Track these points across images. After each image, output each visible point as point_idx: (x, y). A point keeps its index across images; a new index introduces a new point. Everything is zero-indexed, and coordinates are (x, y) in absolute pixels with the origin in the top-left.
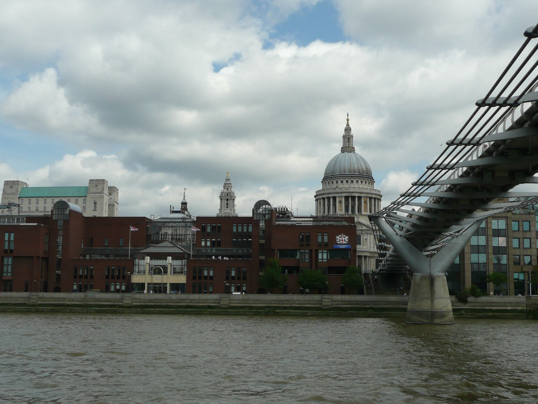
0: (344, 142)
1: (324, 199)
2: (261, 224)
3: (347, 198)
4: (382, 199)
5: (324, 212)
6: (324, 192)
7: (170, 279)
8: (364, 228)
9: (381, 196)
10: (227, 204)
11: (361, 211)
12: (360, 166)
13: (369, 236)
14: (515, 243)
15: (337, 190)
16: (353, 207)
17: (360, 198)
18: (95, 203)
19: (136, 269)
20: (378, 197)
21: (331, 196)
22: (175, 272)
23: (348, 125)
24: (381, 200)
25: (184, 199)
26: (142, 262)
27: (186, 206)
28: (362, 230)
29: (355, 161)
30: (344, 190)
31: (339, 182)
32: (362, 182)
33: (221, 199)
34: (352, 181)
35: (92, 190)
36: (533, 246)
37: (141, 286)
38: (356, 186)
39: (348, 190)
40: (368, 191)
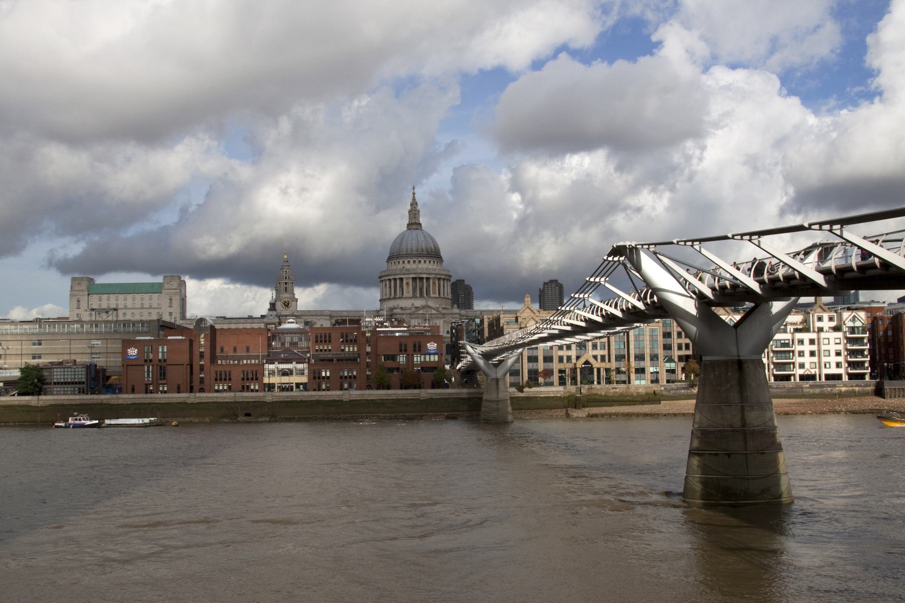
0: (410, 218)
1: (390, 280)
7: (294, 379)
8: (434, 312)
16: (421, 290)
17: (428, 279)
18: (171, 300)
19: (266, 373)
22: (297, 374)
23: (414, 199)
26: (272, 367)
29: (423, 238)
31: (406, 262)
34: (420, 262)
35: (166, 286)
37: (271, 387)
40: (437, 271)
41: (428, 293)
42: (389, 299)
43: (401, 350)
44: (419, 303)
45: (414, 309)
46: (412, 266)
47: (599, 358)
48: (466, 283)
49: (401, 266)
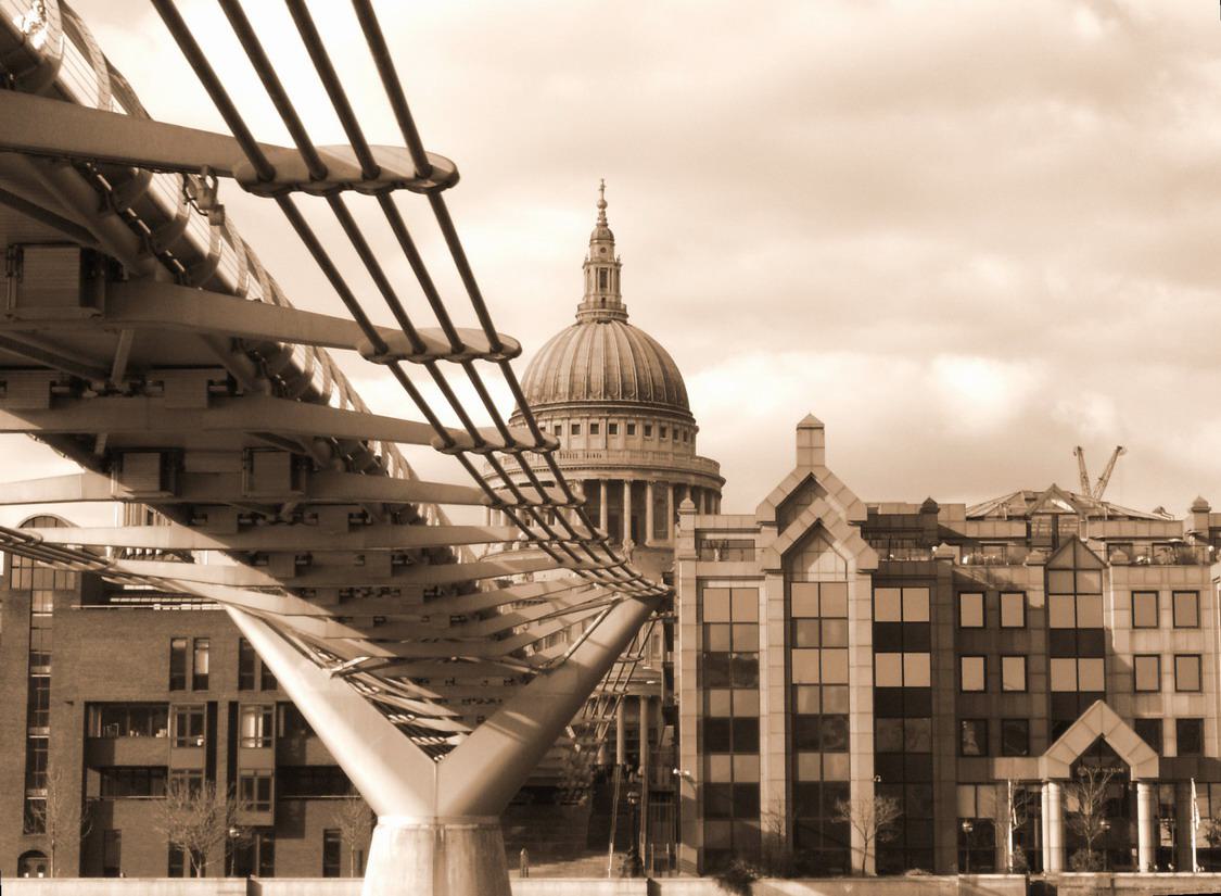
2: (50, 607)
4: (724, 490)
9: (722, 482)
11: (644, 533)
12: (642, 374)
14: (973, 674)
20: (708, 483)
24: (719, 496)
30: (580, 461)
32: (647, 430)
34: (612, 429)
36: (1038, 683)
39: (594, 461)
40: (669, 462)
41: (638, 534)
43: (176, 683)
47: (1169, 730)
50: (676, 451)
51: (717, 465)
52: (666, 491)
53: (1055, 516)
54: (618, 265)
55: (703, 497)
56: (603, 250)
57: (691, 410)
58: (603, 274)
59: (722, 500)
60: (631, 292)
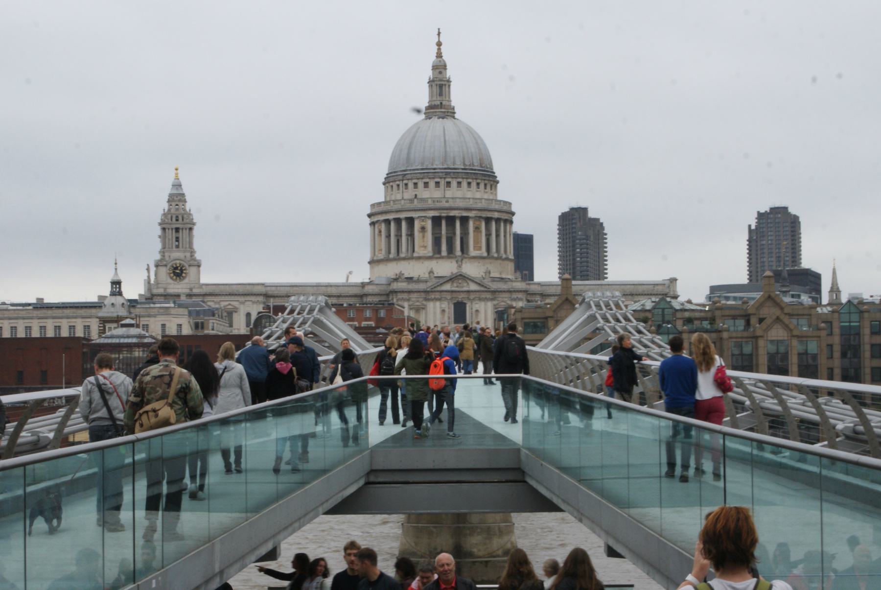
1: (387, 222)
3: (436, 221)
4: (514, 219)
5: (389, 252)
6: (388, 208)
9: (513, 214)
10: (177, 239)
11: (468, 247)
13: (483, 303)
15: (416, 204)
17: (464, 220)
21: (402, 215)
23: (439, 55)
24: (511, 222)
25: (116, 273)
27: (120, 288)
28: (468, 292)
30: (430, 204)
31: (421, 184)
32: (469, 184)
33: (164, 229)
34: (449, 184)
38: (459, 194)
39: (438, 205)
42: (387, 260)
44: (445, 268)
45: (435, 281)
46: (431, 193)
48: (591, 214)
49: (409, 194)
50: (486, 196)
51: (510, 204)
52: (480, 225)
53: (663, 309)
54: (449, 81)
55: (502, 224)
56: (440, 73)
57: (495, 170)
58: (441, 86)
59: (514, 225)
60: (457, 97)
